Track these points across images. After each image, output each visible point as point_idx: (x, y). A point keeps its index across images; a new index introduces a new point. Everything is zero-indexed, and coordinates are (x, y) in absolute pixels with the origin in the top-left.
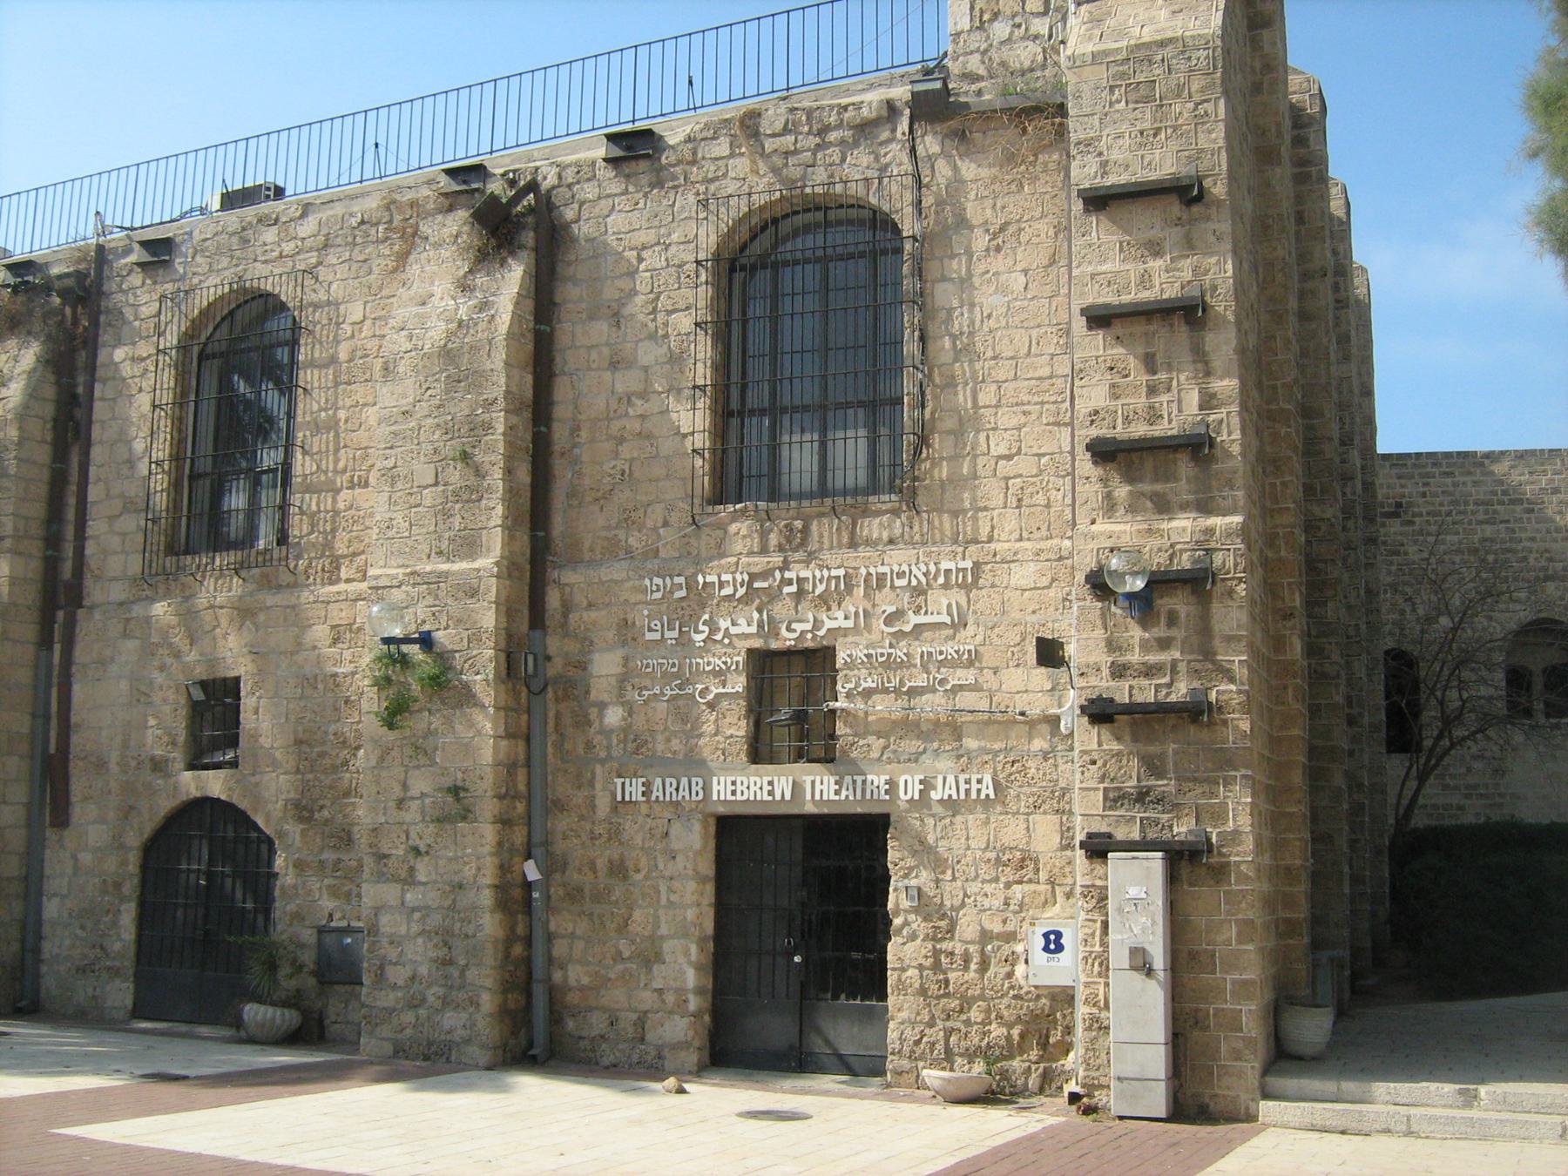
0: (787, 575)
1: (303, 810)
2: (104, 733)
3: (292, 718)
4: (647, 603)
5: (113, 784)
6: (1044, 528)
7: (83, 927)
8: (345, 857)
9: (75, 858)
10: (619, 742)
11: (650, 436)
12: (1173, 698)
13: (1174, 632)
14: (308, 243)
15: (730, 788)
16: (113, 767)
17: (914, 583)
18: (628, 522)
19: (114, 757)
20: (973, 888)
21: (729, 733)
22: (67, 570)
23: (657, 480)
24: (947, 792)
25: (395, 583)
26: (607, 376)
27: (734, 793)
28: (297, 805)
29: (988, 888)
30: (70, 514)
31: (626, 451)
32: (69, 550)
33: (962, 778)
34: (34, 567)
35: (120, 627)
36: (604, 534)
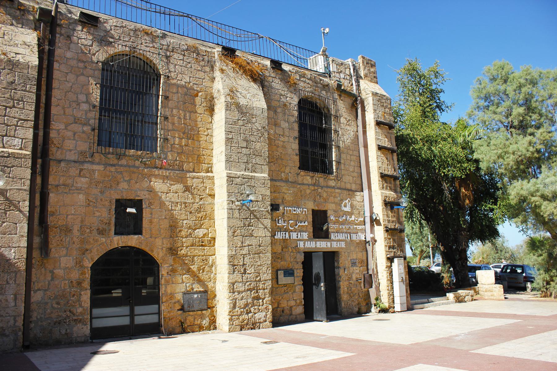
5: (75, 239)
7: (58, 303)
9: (52, 272)
11: (285, 148)
16: (76, 232)
28: (171, 249)
35: (78, 172)
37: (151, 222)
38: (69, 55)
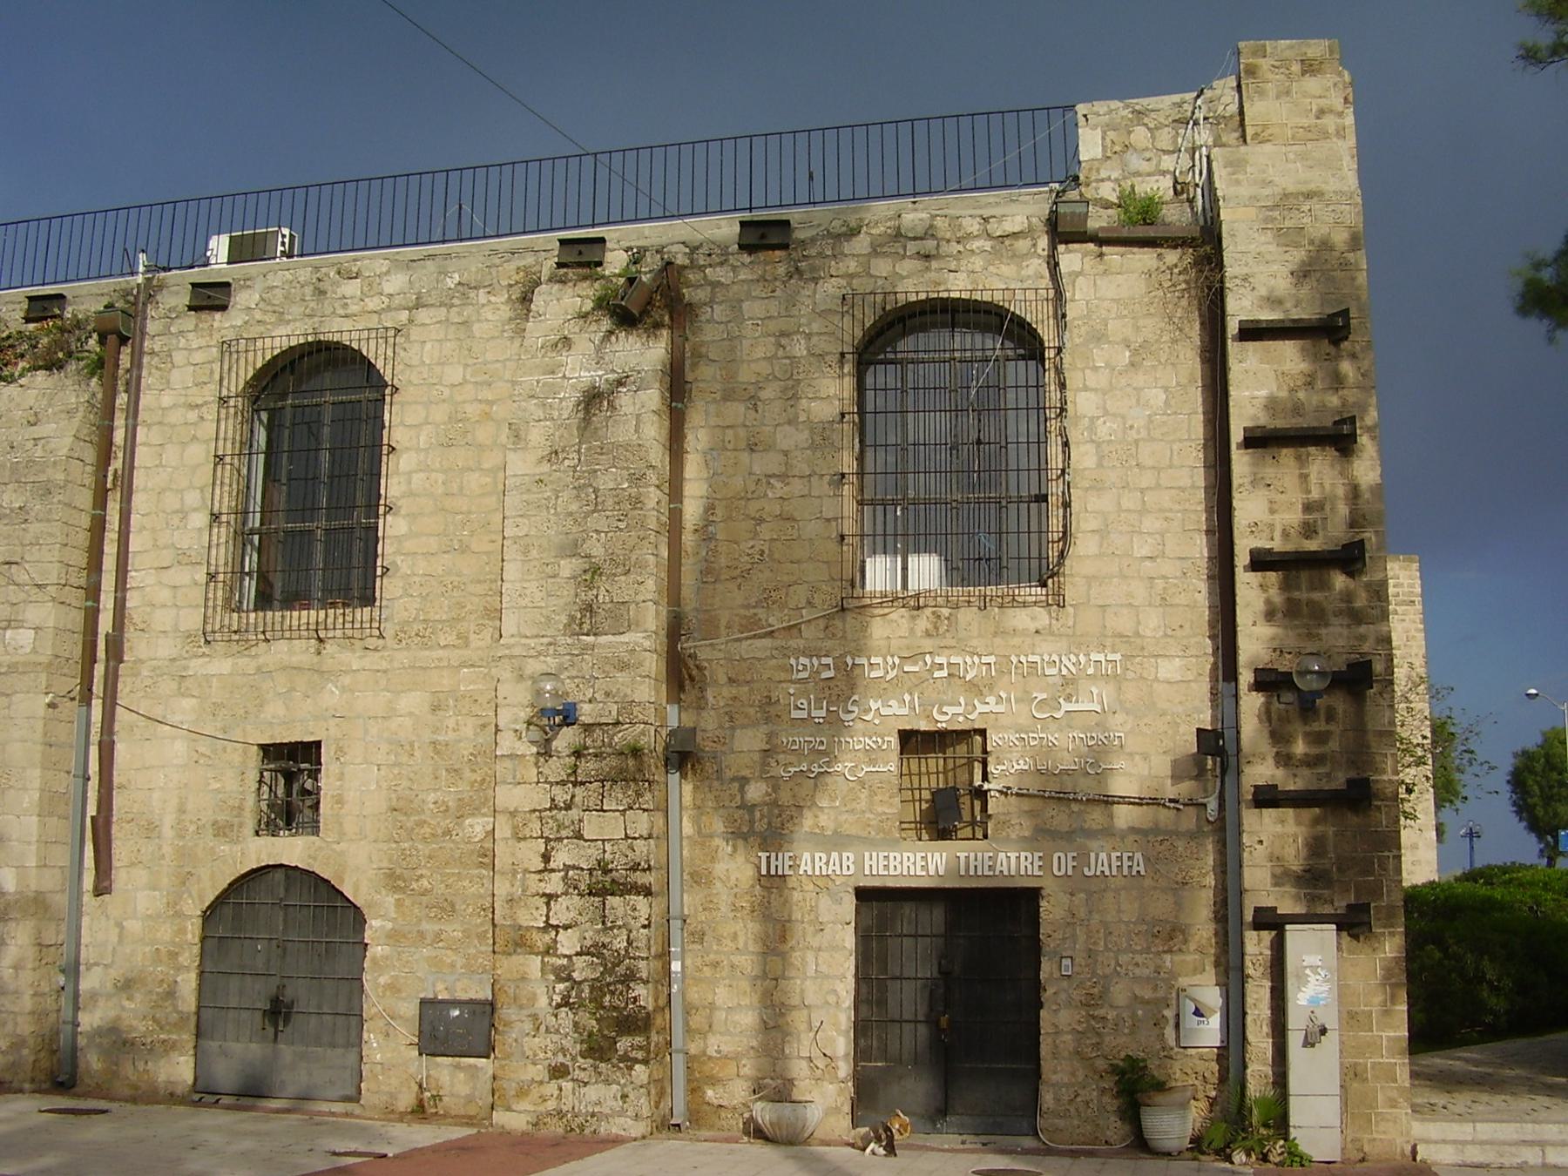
0: (938, 660)
1: (394, 880)
2: (156, 795)
3: (384, 785)
4: (791, 681)
5: (167, 849)
6: (1187, 626)
8: (449, 928)
9: (120, 925)
10: (762, 816)
11: (791, 519)
12: (1333, 786)
13: (1332, 727)
14: (397, 301)
15: (882, 862)
16: (168, 832)
17: (1065, 671)
18: (766, 601)
19: (169, 820)
20: (1123, 958)
21: (880, 810)
22: (105, 624)
23: (798, 562)
24: (1100, 868)
25: (532, 652)
26: (745, 457)
27: (886, 867)
29: (1139, 958)
30: (109, 563)
31: (765, 532)
32: (107, 601)
33: (1114, 855)
34: (77, 619)
35: (174, 685)
36: (742, 612)
37: (340, 800)
38: (167, 400)
